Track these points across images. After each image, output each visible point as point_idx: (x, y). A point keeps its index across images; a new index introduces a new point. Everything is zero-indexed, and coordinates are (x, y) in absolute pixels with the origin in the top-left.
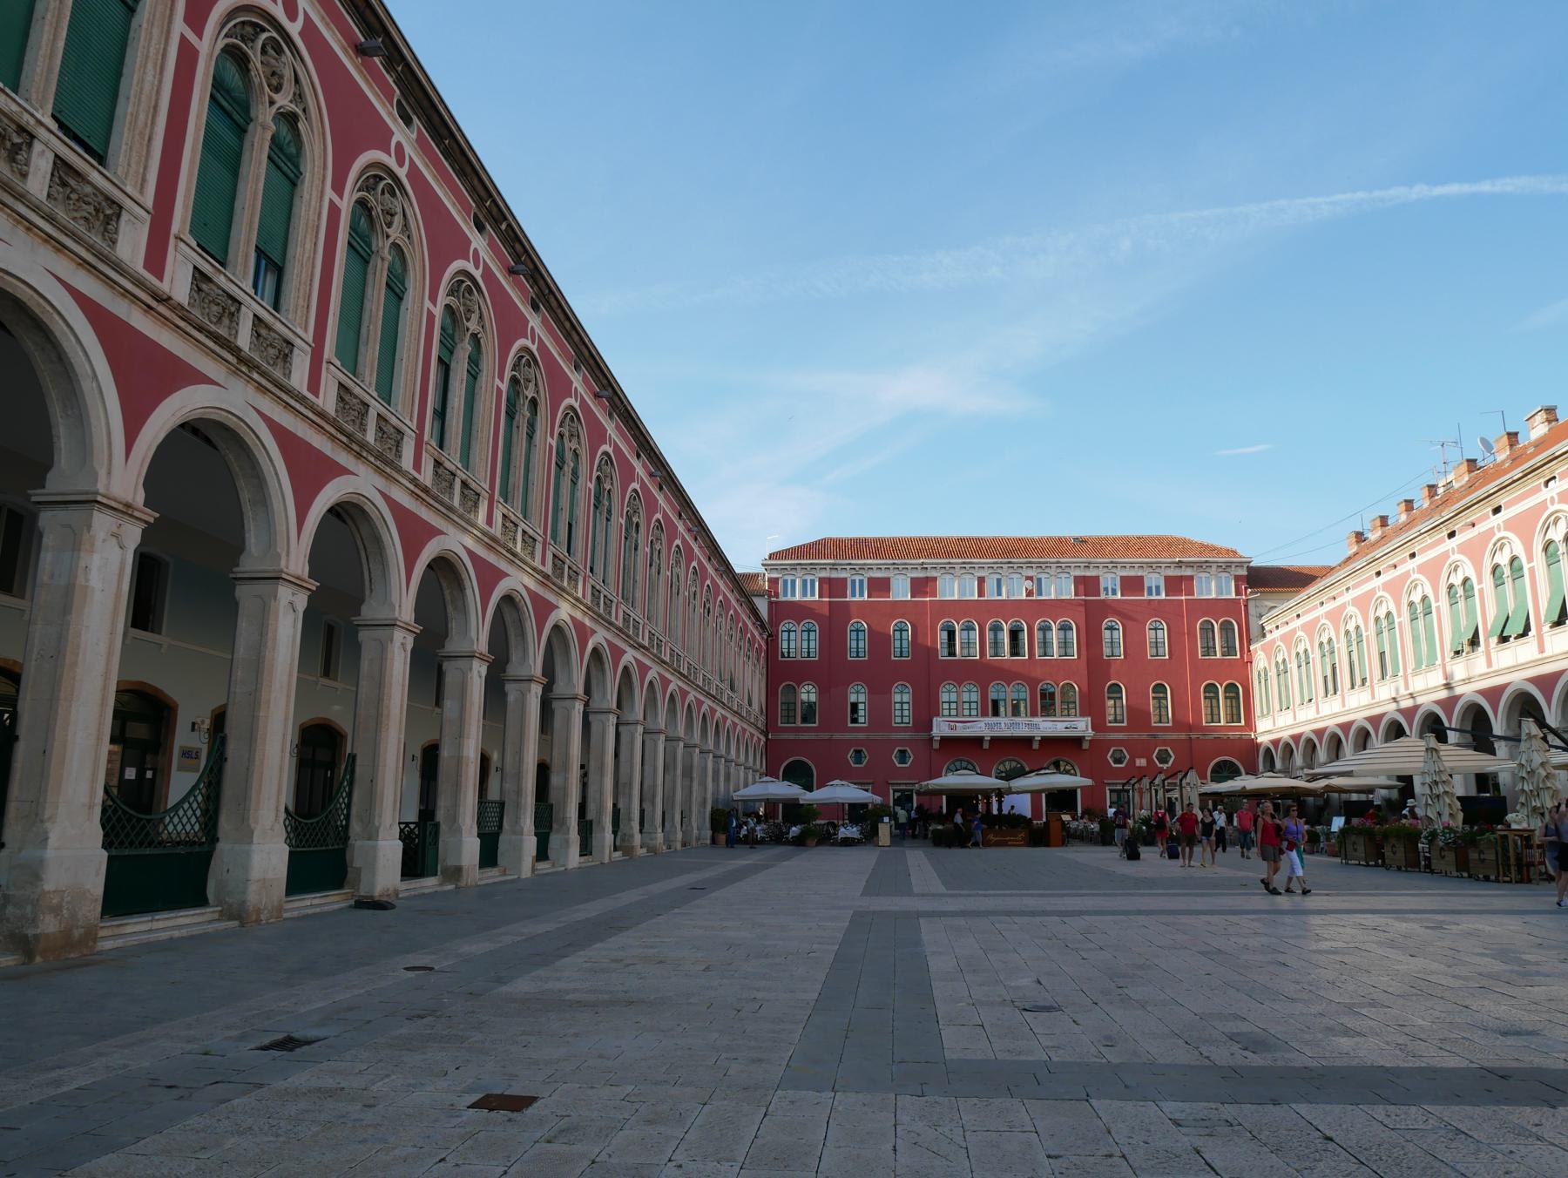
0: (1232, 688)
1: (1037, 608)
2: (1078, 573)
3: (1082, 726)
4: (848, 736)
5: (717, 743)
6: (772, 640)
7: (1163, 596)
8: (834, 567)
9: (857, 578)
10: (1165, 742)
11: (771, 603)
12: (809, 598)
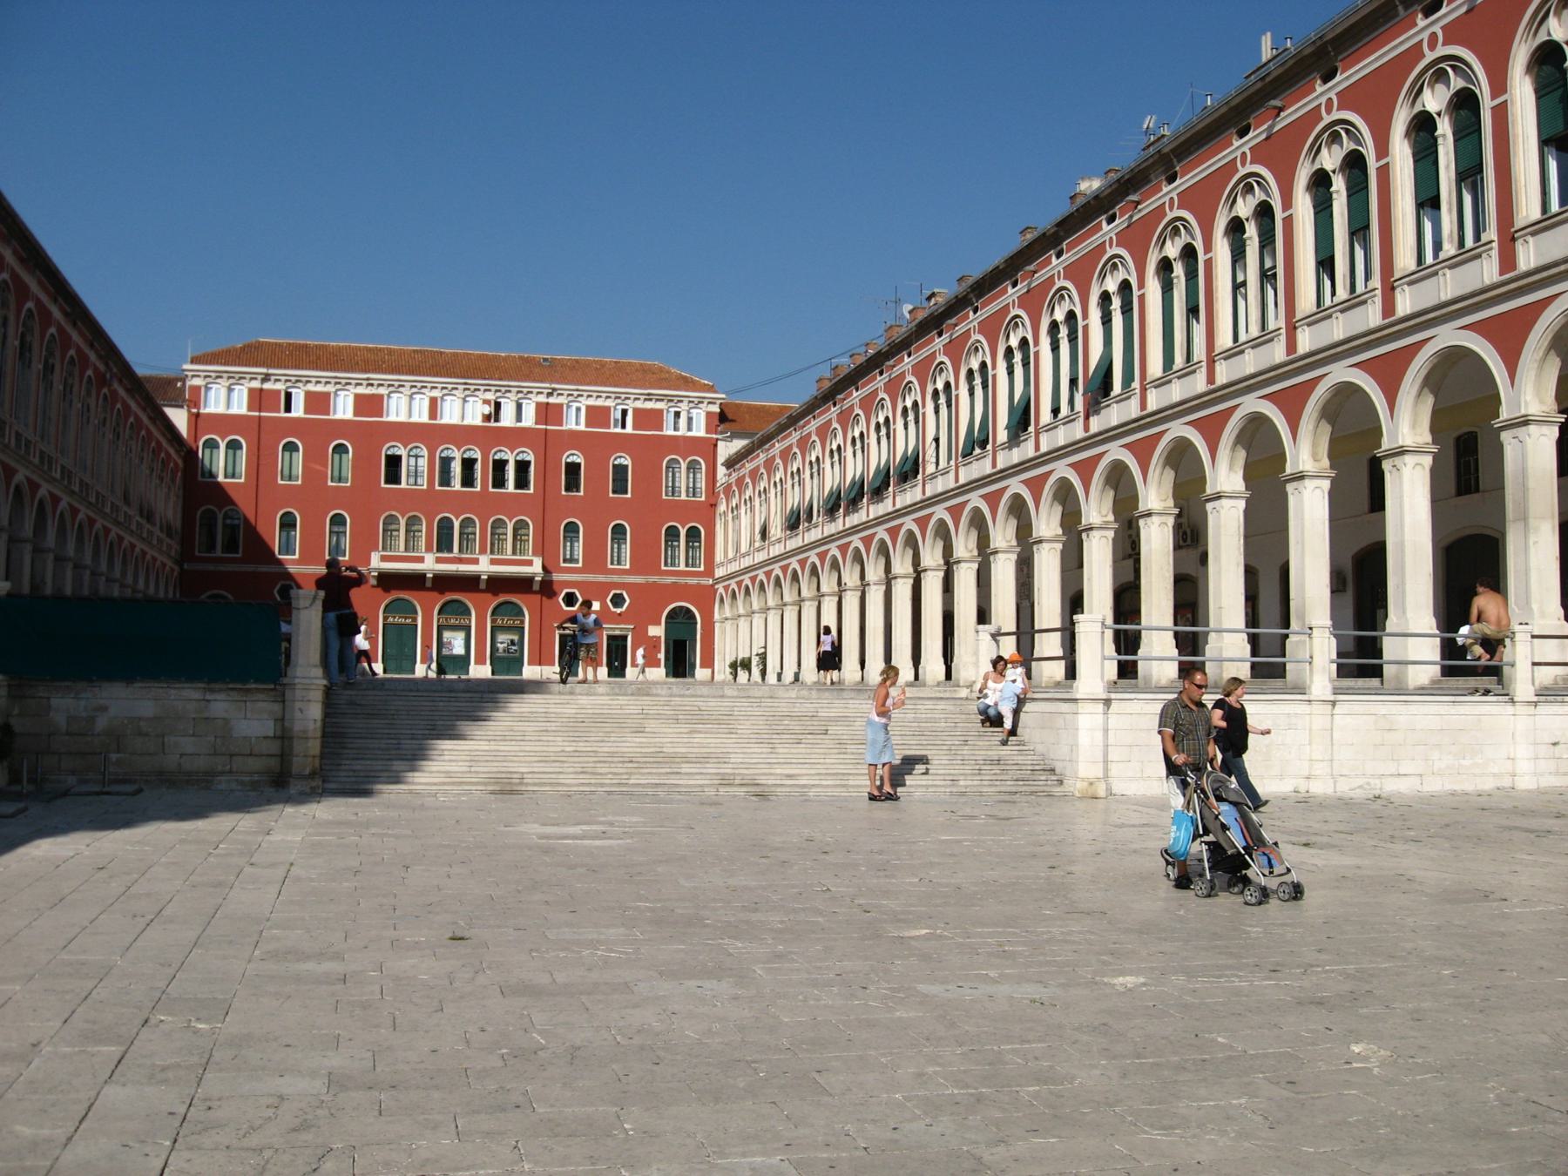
0: (693, 534)
1: (488, 434)
5: (124, 573)
7: (629, 429)
12: (234, 410)
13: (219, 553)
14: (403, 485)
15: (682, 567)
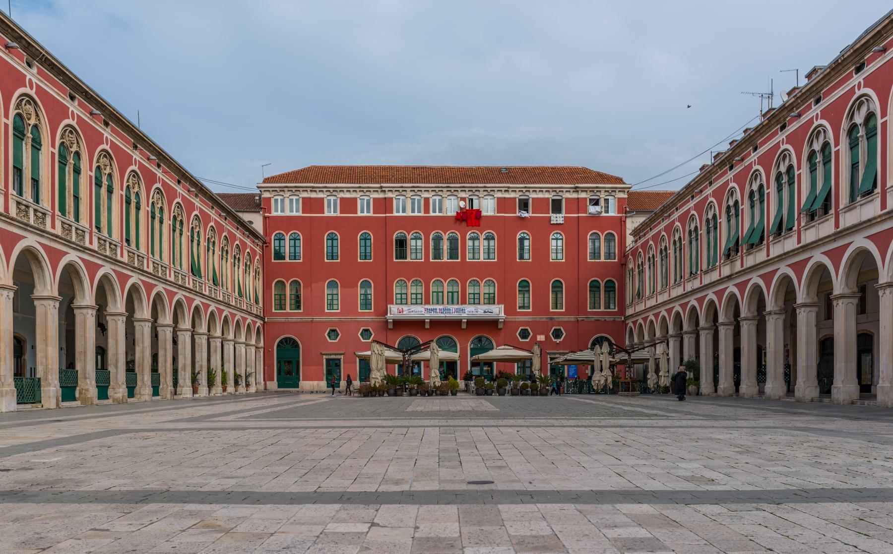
0: (610, 287)
2: (499, 195)
3: (497, 311)
4: (325, 319)
6: (265, 244)
8: (313, 190)
9: (332, 198)
10: (559, 323)
11: (265, 218)
12: (295, 214)
13: (288, 310)
14: (408, 260)
15: (602, 309)
